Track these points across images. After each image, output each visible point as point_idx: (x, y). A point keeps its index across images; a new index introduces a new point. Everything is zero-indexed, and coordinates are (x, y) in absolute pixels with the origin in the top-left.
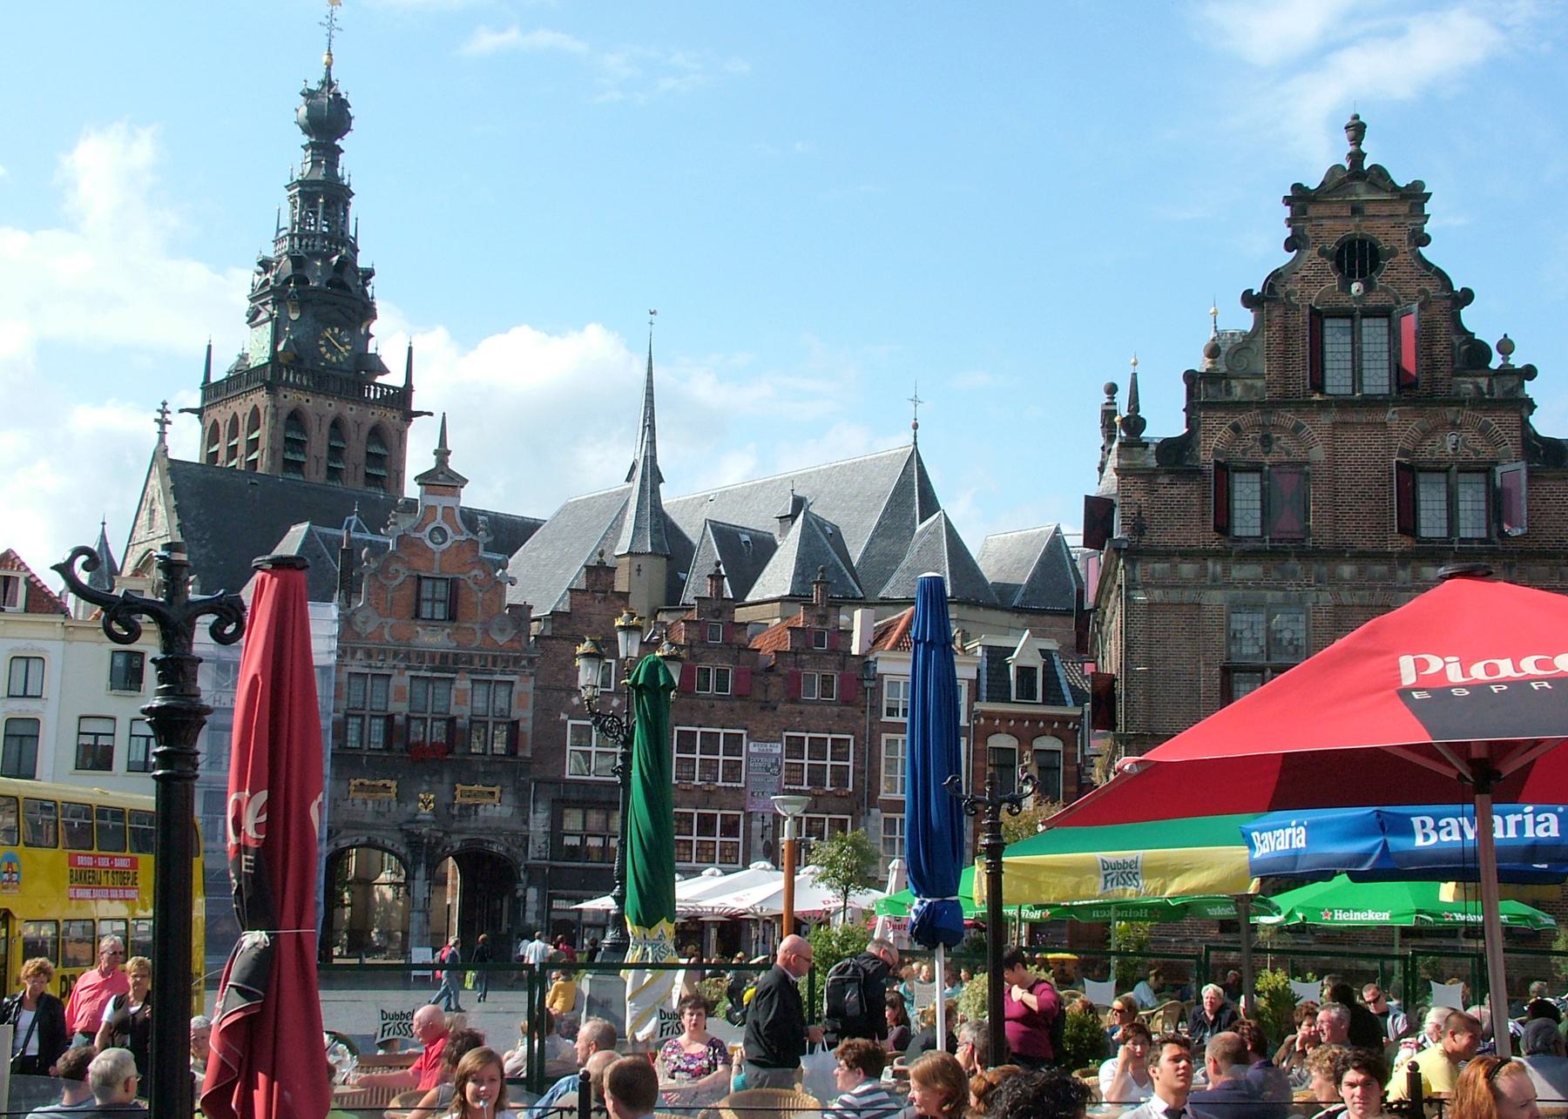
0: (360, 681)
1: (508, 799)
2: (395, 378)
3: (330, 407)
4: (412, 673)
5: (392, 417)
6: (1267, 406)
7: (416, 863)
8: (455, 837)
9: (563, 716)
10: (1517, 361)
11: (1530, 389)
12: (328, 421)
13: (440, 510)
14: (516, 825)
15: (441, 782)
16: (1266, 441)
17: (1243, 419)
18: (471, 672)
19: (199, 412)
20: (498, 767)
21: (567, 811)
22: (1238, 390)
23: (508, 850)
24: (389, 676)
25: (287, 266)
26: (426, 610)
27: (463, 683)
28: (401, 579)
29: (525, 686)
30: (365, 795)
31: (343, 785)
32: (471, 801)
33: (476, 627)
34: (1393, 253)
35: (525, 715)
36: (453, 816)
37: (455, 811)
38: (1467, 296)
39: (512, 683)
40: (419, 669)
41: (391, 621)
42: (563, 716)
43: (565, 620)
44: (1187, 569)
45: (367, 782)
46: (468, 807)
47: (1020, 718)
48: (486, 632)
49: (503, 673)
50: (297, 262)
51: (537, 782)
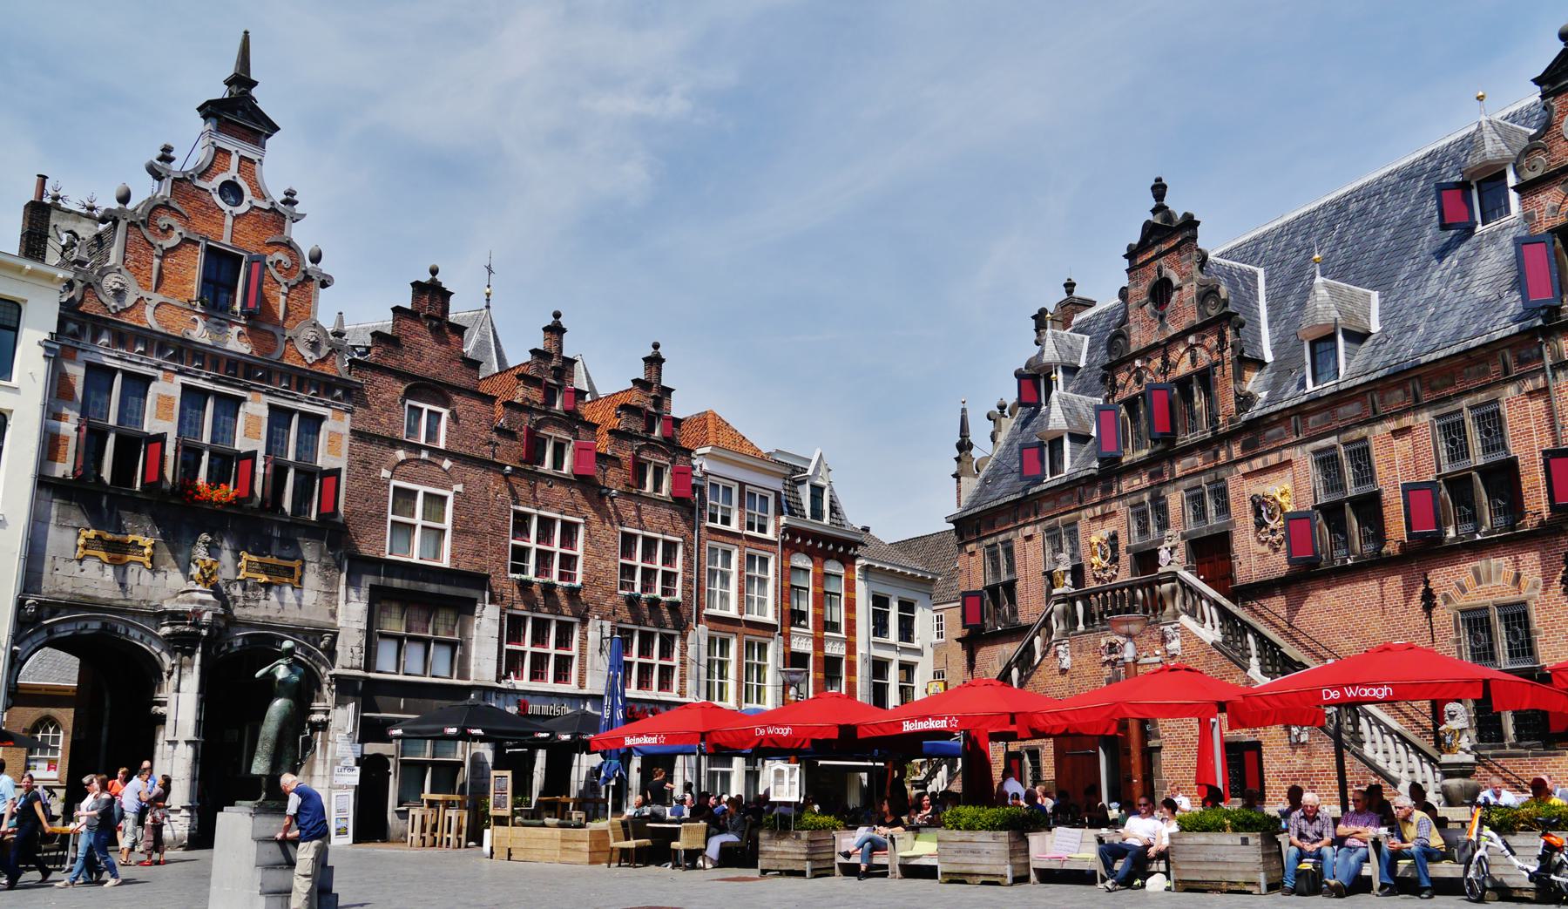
4: (188, 380)
9: (385, 473)
13: (235, 159)
14: (320, 618)
18: (268, 393)
27: (256, 408)
28: (174, 240)
32: (264, 579)
36: (235, 599)
39: (321, 418)
41: (158, 298)
42: (385, 473)
45: (109, 536)
47: (817, 537)
49: (311, 401)
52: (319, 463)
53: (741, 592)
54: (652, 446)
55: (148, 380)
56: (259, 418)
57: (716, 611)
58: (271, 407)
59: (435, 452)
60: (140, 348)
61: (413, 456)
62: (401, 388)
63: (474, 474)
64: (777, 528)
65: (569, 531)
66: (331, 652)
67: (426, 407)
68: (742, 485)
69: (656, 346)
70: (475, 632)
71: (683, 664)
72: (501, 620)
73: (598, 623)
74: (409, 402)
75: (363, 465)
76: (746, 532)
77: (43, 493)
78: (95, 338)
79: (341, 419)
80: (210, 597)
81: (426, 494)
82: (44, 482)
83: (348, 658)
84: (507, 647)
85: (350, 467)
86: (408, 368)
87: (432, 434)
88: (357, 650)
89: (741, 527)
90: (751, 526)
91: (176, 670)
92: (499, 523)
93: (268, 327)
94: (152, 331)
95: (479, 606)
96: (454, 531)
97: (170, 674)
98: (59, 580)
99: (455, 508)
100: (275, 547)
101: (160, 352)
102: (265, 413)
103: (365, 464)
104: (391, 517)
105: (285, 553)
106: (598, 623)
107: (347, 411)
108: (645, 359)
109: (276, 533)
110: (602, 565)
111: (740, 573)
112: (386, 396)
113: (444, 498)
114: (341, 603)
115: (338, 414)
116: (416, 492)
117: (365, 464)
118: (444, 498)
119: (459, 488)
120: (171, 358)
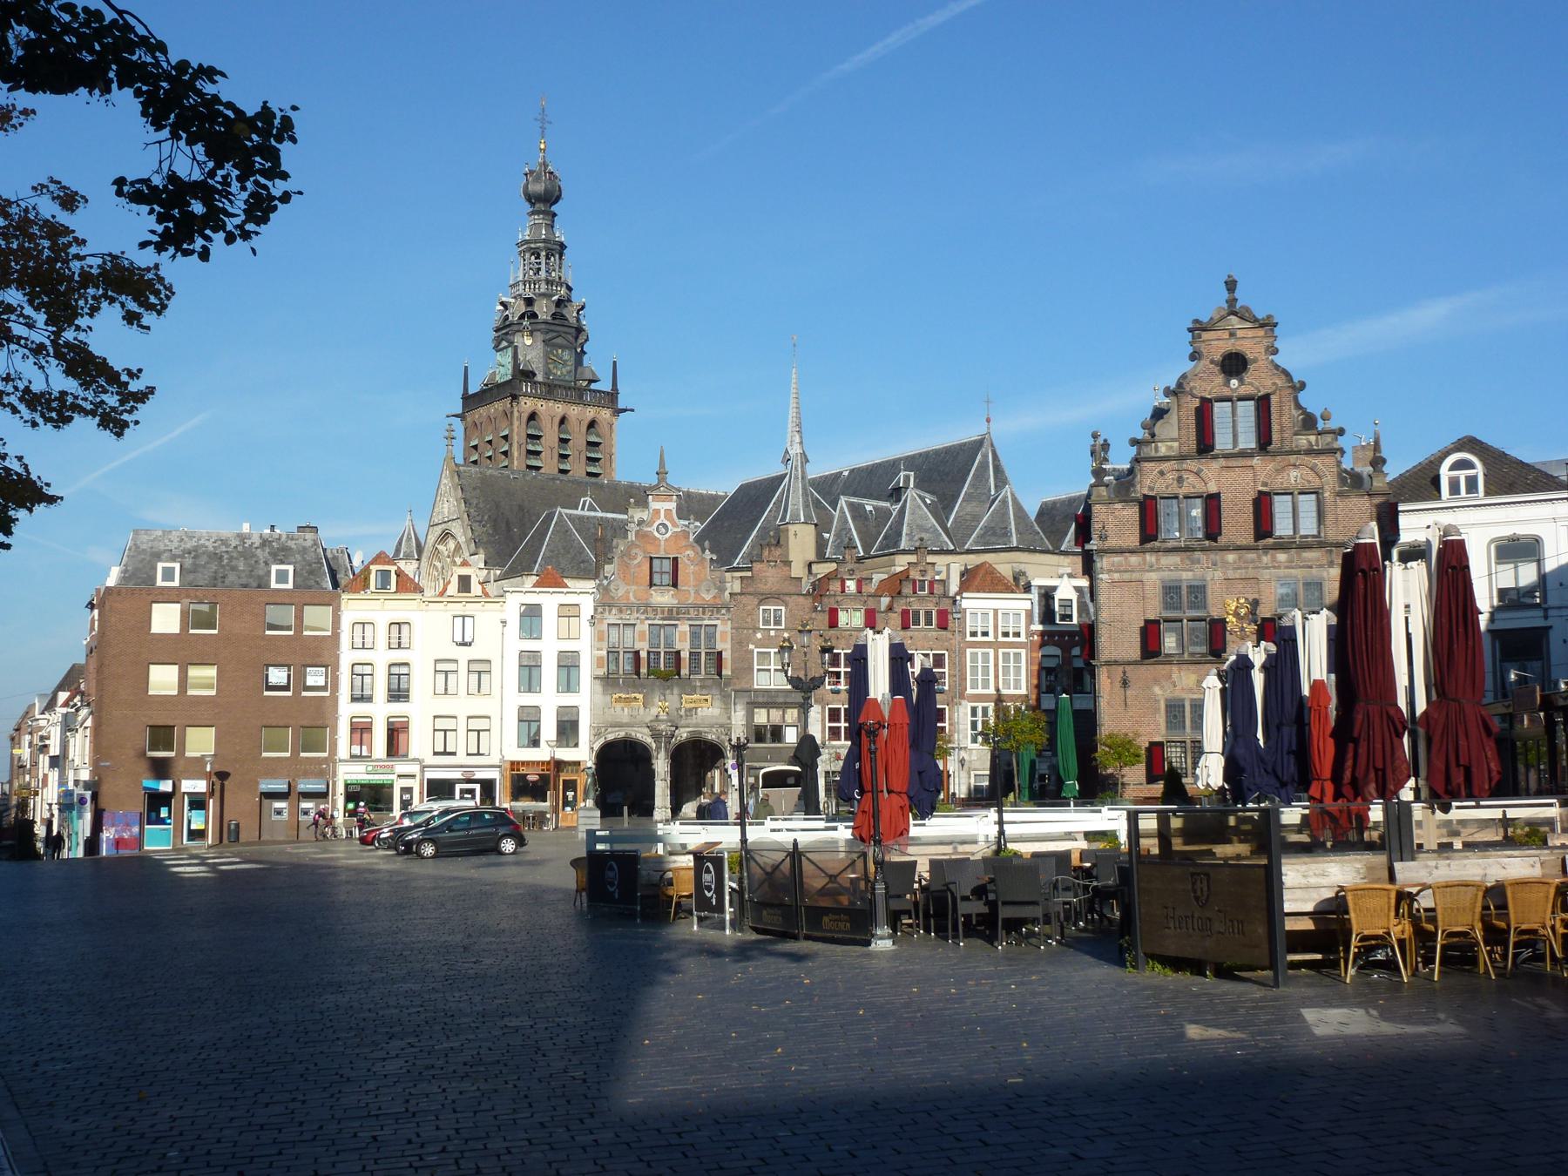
1: (717, 703)
2: (605, 385)
3: (559, 409)
5: (605, 414)
6: (1182, 458)
7: (658, 748)
9: (751, 647)
10: (1333, 424)
11: (1342, 442)
12: (557, 421)
14: (723, 720)
16: (1180, 480)
17: (1166, 466)
19: (462, 416)
22: (1163, 450)
25: (521, 307)
26: (656, 580)
29: (724, 627)
34: (1255, 360)
35: (724, 645)
38: (1303, 385)
42: (751, 647)
44: (1134, 560)
48: (697, 592)
50: (529, 302)
75: (739, 644)
76: (1001, 639)
84: (828, 725)
87: (777, 622)
89: (996, 637)
90: (1006, 634)
103: (740, 643)
111: (996, 665)
117: (740, 643)
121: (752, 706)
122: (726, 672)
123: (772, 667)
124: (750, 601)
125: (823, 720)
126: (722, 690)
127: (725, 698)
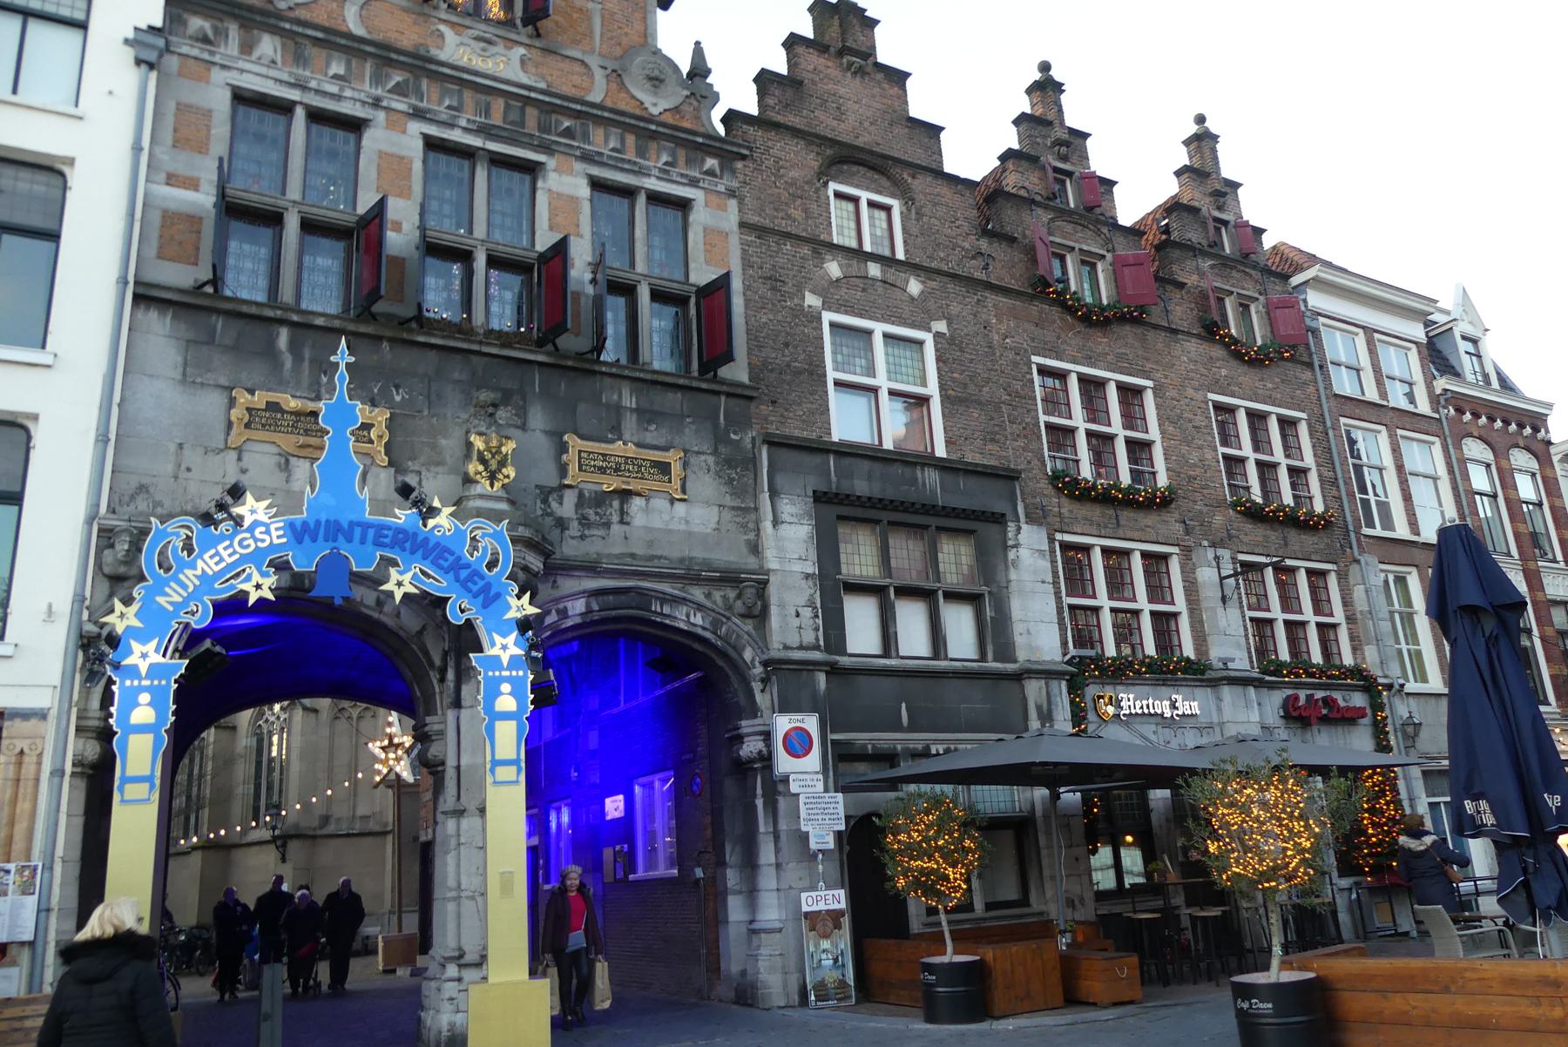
0: (269, 122)
1: (705, 485)
8: (569, 585)
9: (812, 300)
14: (731, 554)
15: (523, 427)
18: (587, 158)
20: (673, 400)
21: (843, 530)
23: (716, 624)
24: (355, 126)
27: (565, 182)
30: (289, 442)
31: (212, 402)
33: (594, 62)
36: (561, 524)
37: (567, 507)
39: (683, 205)
40: (452, 126)
42: (812, 300)
43: (790, 93)
45: (293, 404)
46: (601, 499)
48: (617, 76)
49: (664, 175)
51: (774, 443)
52: (693, 279)
53: (1407, 498)
54: (1225, 264)
55: (355, 126)
56: (574, 200)
57: (1378, 531)
58: (597, 185)
59: (888, 261)
60: (337, 68)
61: (854, 271)
62: (812, 161)
63: (961, 303)
64: (1435, 400)
65: (1130, 395)
66: (759, 615)
67: (865, 196)
68: (1369, 331)
69: (1200, 119)
70: (1013, 575)
71: (1350, 619)
72: (1052, 552)
73: (1210, 554)
74: (833, 186)
77: (158, 324)
78: (247, 48)
79: (724, 208)
80: (503, 506)
81: (886, 336)
82: (146, 296)
83: (791, 623)
85: (747, 288)
86: (821, 130)
88: (807, 613)
91: (451, 663)
92: (1018, 386)
93: (578, 55)
94: (349, 36)
95: (1011, 527)
96: (945, 398)
97: (443, 671)
98: (193, 488)
99: (939, 359)
100: (630, 424)
101: (377, 80)
102: (584, 191)
103: (774, 281)
104: (831, 375)
105: (649, 438)
106: (1210, 554)
107: (731, 193)
108: (1187, 143)
109: (629, 401)
110: (1194, 458)
112: (792, 174)
113: (921, 343)
114: (767, 525)
115: (714, 198)
116: (869, 333)
118: (921, 343)
119: (941, 326)
120: (399, 90)
121: (837, 509)
122: (737, 372)
123: (882, 381)
124: (800, 161)
125: (1056, 583)
126: (719, 438)
127: (736, 468)
